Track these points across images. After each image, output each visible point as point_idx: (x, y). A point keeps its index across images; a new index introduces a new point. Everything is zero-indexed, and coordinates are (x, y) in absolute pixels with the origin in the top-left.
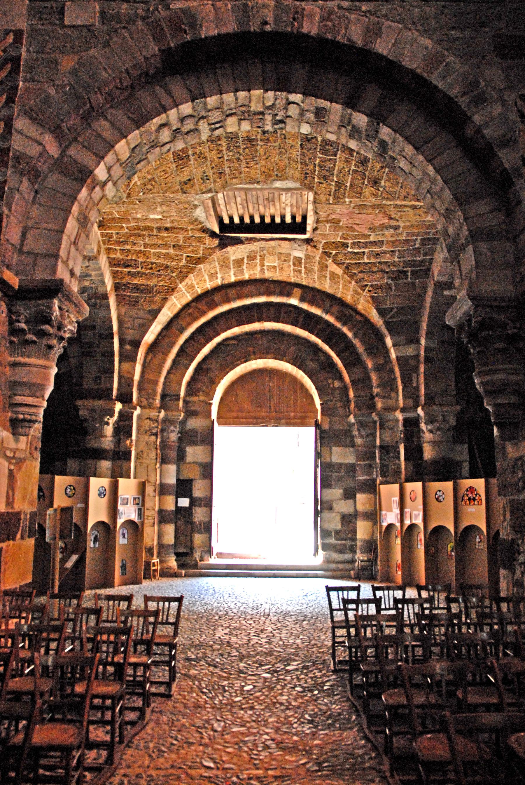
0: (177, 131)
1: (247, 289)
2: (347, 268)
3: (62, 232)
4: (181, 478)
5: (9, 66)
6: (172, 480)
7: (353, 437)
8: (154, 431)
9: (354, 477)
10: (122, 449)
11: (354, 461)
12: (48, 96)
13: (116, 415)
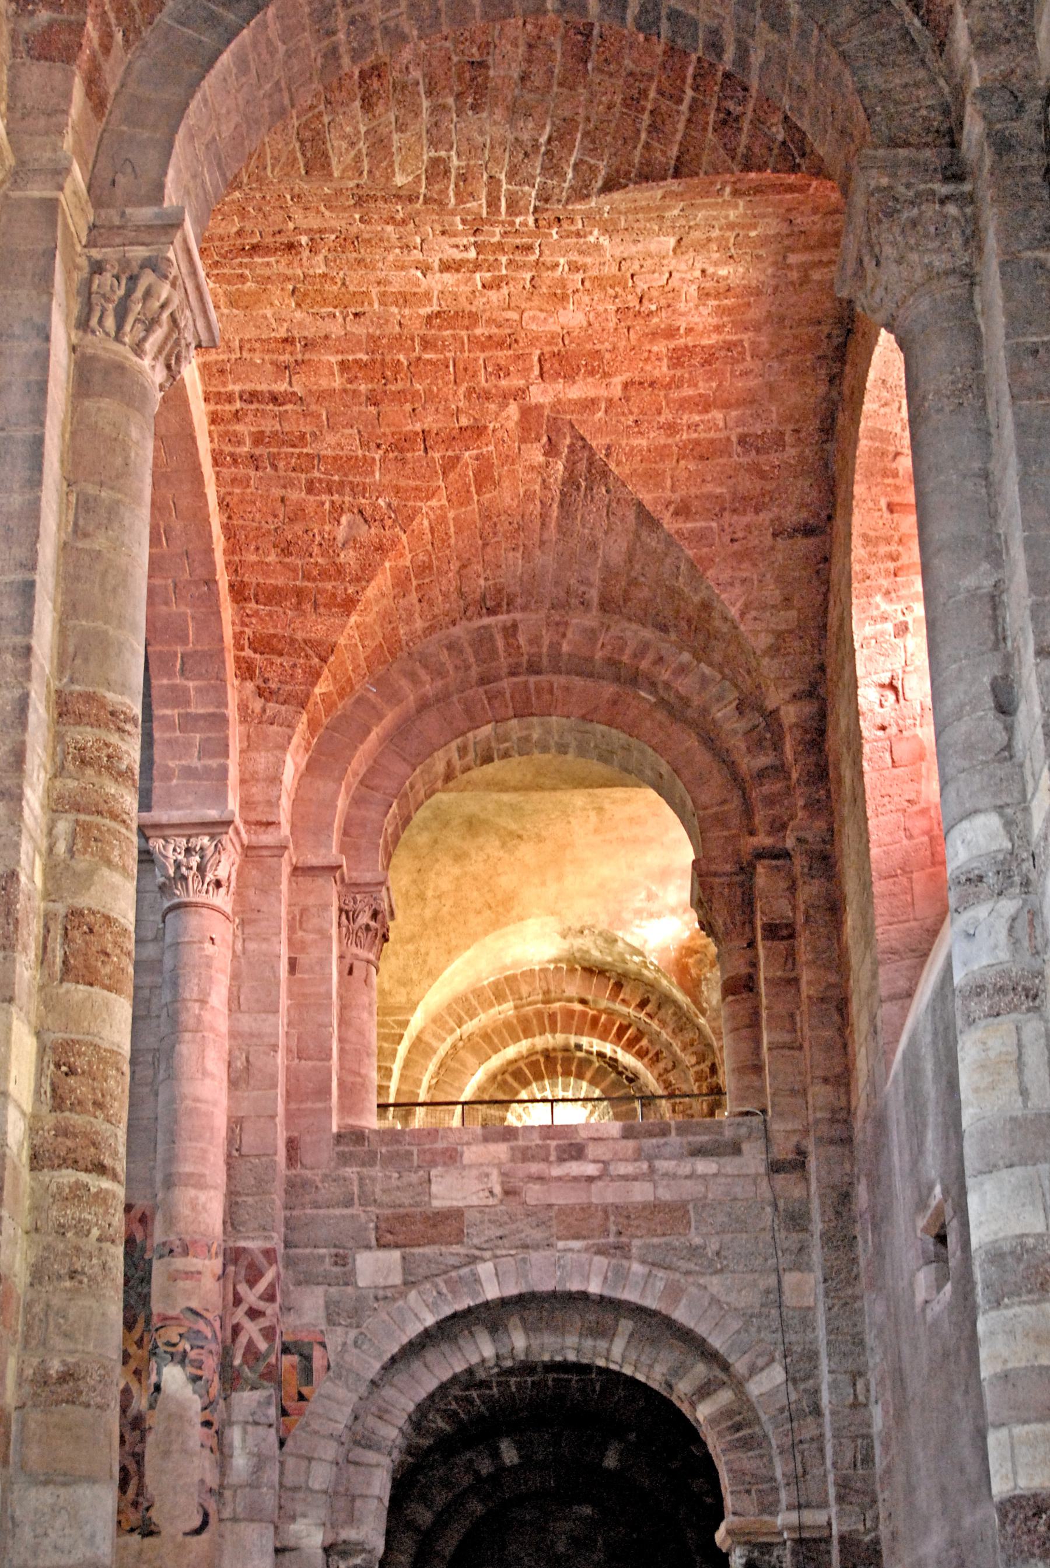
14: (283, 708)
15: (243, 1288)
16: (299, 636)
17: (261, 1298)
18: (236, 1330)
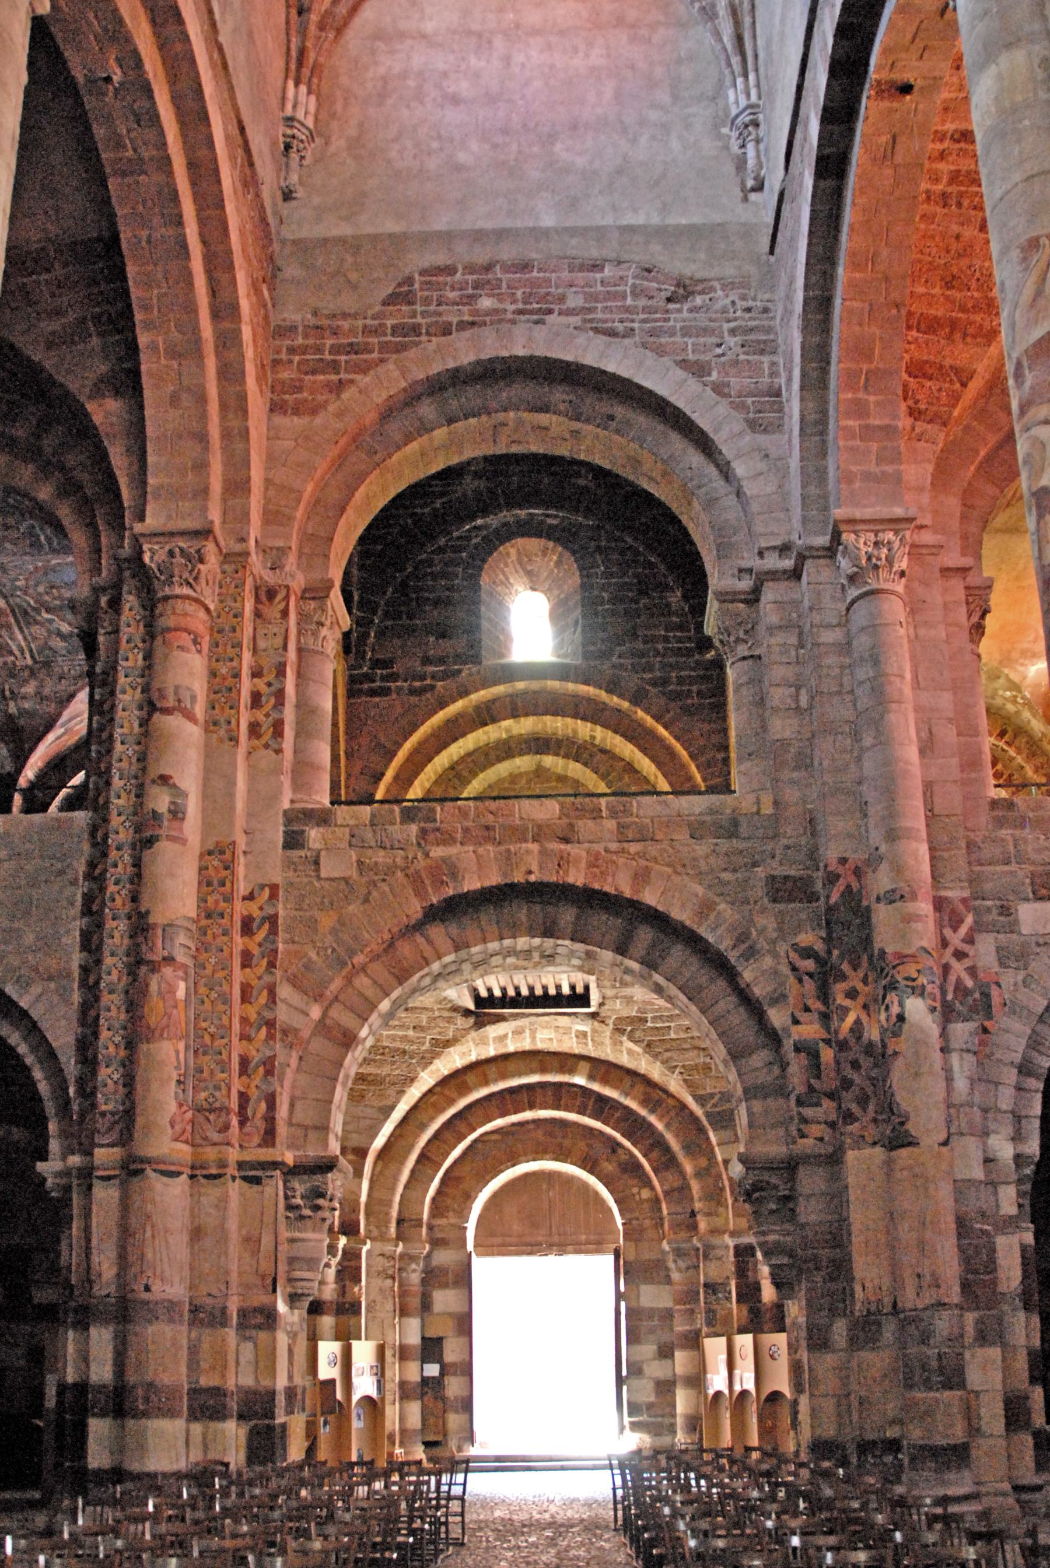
0: (440, 974)
1: (511, 1066)
2: (649, 1045)
3: (331, 1102)
4: (427, 1335)
5: (267, 926)
6: (414, 1339)
7: (667, 1269)
8: (390, 1272)
9: (672, 1330)
10: (348, 1298)
11: (669, 1304)
12: (310, 960)
13: (340, 1253)
14: (929, 426)
15: (948, 932)
16: (947, 362)
17: (963, 941)
18: (946, 968)
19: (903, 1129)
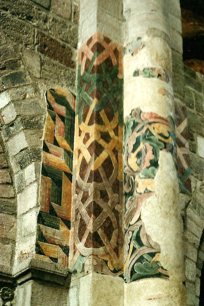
19: (156, 258)
